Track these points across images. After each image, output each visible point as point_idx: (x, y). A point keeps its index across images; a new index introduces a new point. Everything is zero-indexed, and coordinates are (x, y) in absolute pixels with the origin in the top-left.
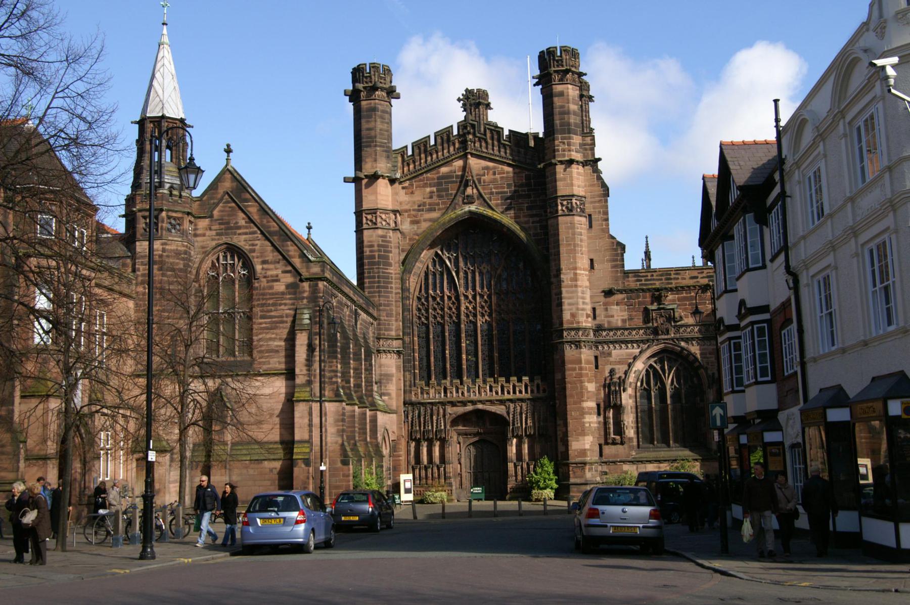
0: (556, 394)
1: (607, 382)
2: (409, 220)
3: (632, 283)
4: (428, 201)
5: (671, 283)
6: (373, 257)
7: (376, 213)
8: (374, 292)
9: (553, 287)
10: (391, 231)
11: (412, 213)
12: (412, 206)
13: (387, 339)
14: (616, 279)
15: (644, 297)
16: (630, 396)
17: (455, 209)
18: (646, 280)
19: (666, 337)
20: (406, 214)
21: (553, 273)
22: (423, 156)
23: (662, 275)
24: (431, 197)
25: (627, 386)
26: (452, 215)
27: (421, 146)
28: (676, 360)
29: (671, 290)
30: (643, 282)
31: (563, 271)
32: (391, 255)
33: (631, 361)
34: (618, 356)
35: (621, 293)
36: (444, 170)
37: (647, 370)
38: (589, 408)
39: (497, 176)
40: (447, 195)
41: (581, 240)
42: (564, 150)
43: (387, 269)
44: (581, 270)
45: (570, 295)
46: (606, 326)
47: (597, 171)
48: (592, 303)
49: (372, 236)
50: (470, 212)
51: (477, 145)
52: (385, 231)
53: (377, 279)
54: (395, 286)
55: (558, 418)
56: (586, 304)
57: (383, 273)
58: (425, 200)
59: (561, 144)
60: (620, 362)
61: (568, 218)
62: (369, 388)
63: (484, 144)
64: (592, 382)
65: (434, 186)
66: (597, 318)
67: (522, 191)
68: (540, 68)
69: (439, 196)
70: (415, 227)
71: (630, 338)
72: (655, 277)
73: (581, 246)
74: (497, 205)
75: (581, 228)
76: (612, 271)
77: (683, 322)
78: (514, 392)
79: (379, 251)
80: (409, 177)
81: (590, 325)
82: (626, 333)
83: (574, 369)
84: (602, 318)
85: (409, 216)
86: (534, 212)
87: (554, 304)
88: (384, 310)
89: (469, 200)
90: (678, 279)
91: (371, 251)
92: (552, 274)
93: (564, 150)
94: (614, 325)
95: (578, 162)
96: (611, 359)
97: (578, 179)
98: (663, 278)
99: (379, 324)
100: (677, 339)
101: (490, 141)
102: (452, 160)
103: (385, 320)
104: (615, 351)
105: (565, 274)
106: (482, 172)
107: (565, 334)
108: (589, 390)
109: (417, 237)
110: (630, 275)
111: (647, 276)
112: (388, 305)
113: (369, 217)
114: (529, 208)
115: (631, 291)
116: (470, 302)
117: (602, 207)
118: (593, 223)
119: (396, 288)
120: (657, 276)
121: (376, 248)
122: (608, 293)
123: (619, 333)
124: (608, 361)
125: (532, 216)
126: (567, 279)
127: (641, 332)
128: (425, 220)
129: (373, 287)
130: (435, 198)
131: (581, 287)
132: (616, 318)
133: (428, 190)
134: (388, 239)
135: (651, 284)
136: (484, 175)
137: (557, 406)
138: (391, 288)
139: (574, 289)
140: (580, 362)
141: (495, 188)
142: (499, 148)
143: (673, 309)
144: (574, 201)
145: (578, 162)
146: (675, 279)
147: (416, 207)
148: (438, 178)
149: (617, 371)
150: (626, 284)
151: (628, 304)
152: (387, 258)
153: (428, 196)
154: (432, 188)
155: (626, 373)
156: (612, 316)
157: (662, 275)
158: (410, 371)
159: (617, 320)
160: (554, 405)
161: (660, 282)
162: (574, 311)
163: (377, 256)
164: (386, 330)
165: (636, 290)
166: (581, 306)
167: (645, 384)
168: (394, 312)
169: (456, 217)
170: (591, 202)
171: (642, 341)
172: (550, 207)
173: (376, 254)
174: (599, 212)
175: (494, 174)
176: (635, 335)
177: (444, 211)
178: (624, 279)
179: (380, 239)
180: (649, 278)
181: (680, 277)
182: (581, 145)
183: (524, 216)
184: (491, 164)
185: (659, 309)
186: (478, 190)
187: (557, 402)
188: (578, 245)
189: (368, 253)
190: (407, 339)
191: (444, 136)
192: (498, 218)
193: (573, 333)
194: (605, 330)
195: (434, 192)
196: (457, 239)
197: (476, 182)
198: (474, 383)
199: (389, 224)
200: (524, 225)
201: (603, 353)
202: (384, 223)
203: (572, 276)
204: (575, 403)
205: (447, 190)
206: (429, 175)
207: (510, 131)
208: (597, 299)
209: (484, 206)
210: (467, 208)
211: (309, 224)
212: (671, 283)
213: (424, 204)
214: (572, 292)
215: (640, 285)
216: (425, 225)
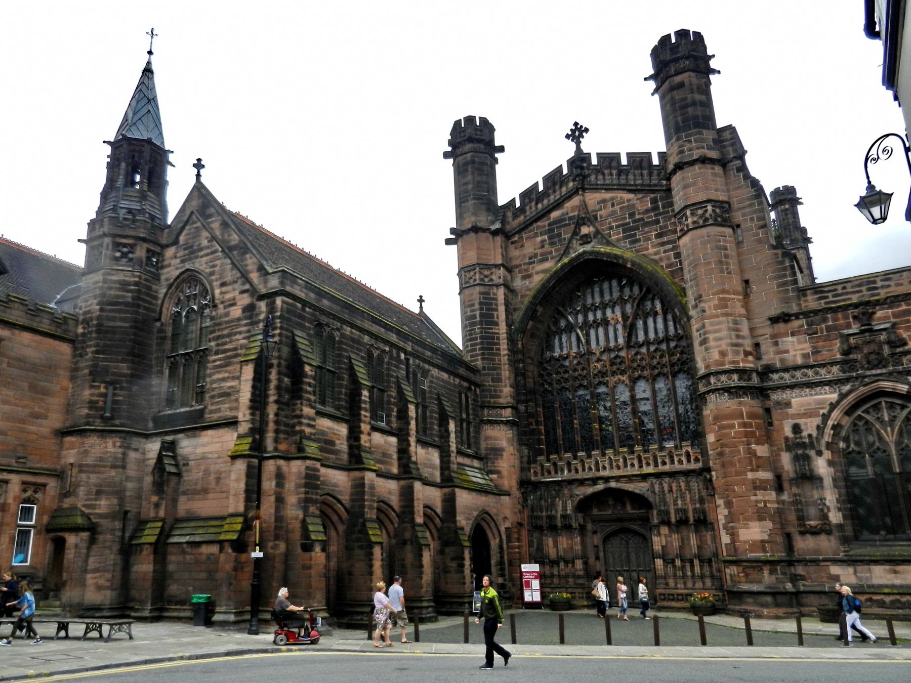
0: (711, 465)
1: (791, 443)
2: (520, 276)
3: (812, 302)
4: (539, 251)
5: (878, 294)
6: (474, 317)
7: (475, 269)
8: (477, 355)
9: (693, 321)
10: (495, 288)
11: (523, 267)
12: (522, 260)
13: (494, 407)
14: (787, 301)
15: (834, 320)
16: (830, 463)
17: (569, 253)
18: (834, 296)
19: (879, 371)
20: (517, 270)
21: (691, 303)
22: (533, 204)
23: (860, 285)
24: (543, 247)
25: (823, 449)
26: (566, 260)
27: (529, 195)
28: (903, 407)
29: (878, 303)
30: (831, 299)
31: (704, 298)
32: (495, 313)
33: (825, 411)
34: (802, 405)
35: (797, 318)
36: (555, 215)
37: (855, 425)
38: (762, 481)
39: (617, 208)
40: (560, 241)
41: (726, 256)
42: (691, 150)
43: (492, 329)
44: (728, 292)
45: (717, 327)
46: (778, 365)
47: (743, 168)
48: (753, 337)
49: (472, 294)
50: (584, 252)
51: (593, 178)
52: (487, 288)
53: (479, 341)
54: (504, 346)
55: (716, 496)
56: (743, 337)
57: (486, 333)
58: (536, 251)
59: (686, 143)
60: (808, 414)
61: (704, 231)
62: (445, 459)
63: (600, 177)
64: (763, 444)
65: (545, 234)
66: (764, 357)
67: (648, 218)
68: (654, 67)
69: (552, 244)
70: (527, 282)
71: (817, 379)
72: (848, 290)
73: (727, 264)
74: (618, 240)
75: (725, 241)
76: (779, 292)
77: (907, 348)
78: (656, 465)
79: (481, 309)
80: (518, 229)
81: (752, 365)
82: (810, 372)
83: (733, 426)
84: (770, 356)
85: (520, 272)
86: (665, 239)
87: (696, 343)
88: (488, 375)
89: (586, 239)
90: (889, 286)
91: (472, 311)
92: (690, 306)
93: (691, 150)
94: (790, 363)
95: (712, 161)
96: (790, 411)
97: (713, 181)
98: (864, 288)
99: (482, 391)
100: (900, 373)
101: (606, 172)
102: (563, 201)
103: (490, 386)
104: (797, 399)
105: (705, 302)
106: (598, 207)
107: (712, 380)
108: (759, 454)
109: (528, 293)
110: (808, 292)
111: (835, 290)
112: (494, 369)
113: (472, 273)
114: (659, 236)
115: (816, 312)
116: (599, 360)
117: (755, 212)
118: (744, 234)
119: (504, 350)
120: (852, 287)
121: (477, 306)
122: (774, 320)
123: (798, 374)
124: (787, 414)
125: (663, 244)
126: (710, 307)
127: (835, 369)
128: (537, 273)
129: (475, 350)
130: (547, 246)
131: (730, 315)
132: (792, 353)
133: (539, 239)
134: (492, 296)
135: (844, 300)
136: (601, 210)
137: (714, 478)
138: (499, 349)
139: (721, 319)
140: (741, 416)
141: (614, 221)
142: (619, 175)
143: (884, 330)
144: (710, 208)
145: (712, 161)
146: (882, 287)
147: (527, 261)
148: (549, 225)
149: (803, 427)
150: (803, 305)
151: (809, 332)
152: (492, 316)
153: (539, 246)
154: (543, 237)
155: (818, 427)
156: (787, 352)
157: (860, 285)
158: (525, 444)
159: (795, 356)
160: (711, 480)
161: (857, 295)
162: (724, 347)
163: (478, 316)
164: (492, 397)
165: (820, 310)
166: (735, 341)
167: (852, 445)
168: (503, 379)
169: (570, 262)
170: (739, 209)
171: (839, 380)
172: (680, 223)
173: (478, 313)
174: (752, 219)
175: (613, 205)
176: (825, 374)
177: (558, 259)
178: (799, 298)
179: (482, 296)
180: (840, 291)
181: (892, 283)
182: (714, 140)
183: (653, 247)
184: (608, 195)
185: (862, 332)
186: (594, 226)
187: (713, 473)
188: (721, 262)
189: (469, 314)
190: (522, 408)
191: (554, 179)
192: (619, 253)
193: (723, 378)
194: (777, 371)
195: (545, 241)
196: (579, 292)
197: (593, 219)
198: (604, 455)
199: (491, 280)
200: (653, 257)
201: (778, 403)
202: (486, 280)
203: (716, 302)
204: (738, 473)
205: (560, 235)
206: (539, 223)
207: (629, 155)
208: (760, 332)
209: (601, 244)
210: (581, 250)
211: (421, 297)
212: (878, 294)
213: (536, 255)
214: (719, 323)
215: (826, 303)
216: (537, 280)
